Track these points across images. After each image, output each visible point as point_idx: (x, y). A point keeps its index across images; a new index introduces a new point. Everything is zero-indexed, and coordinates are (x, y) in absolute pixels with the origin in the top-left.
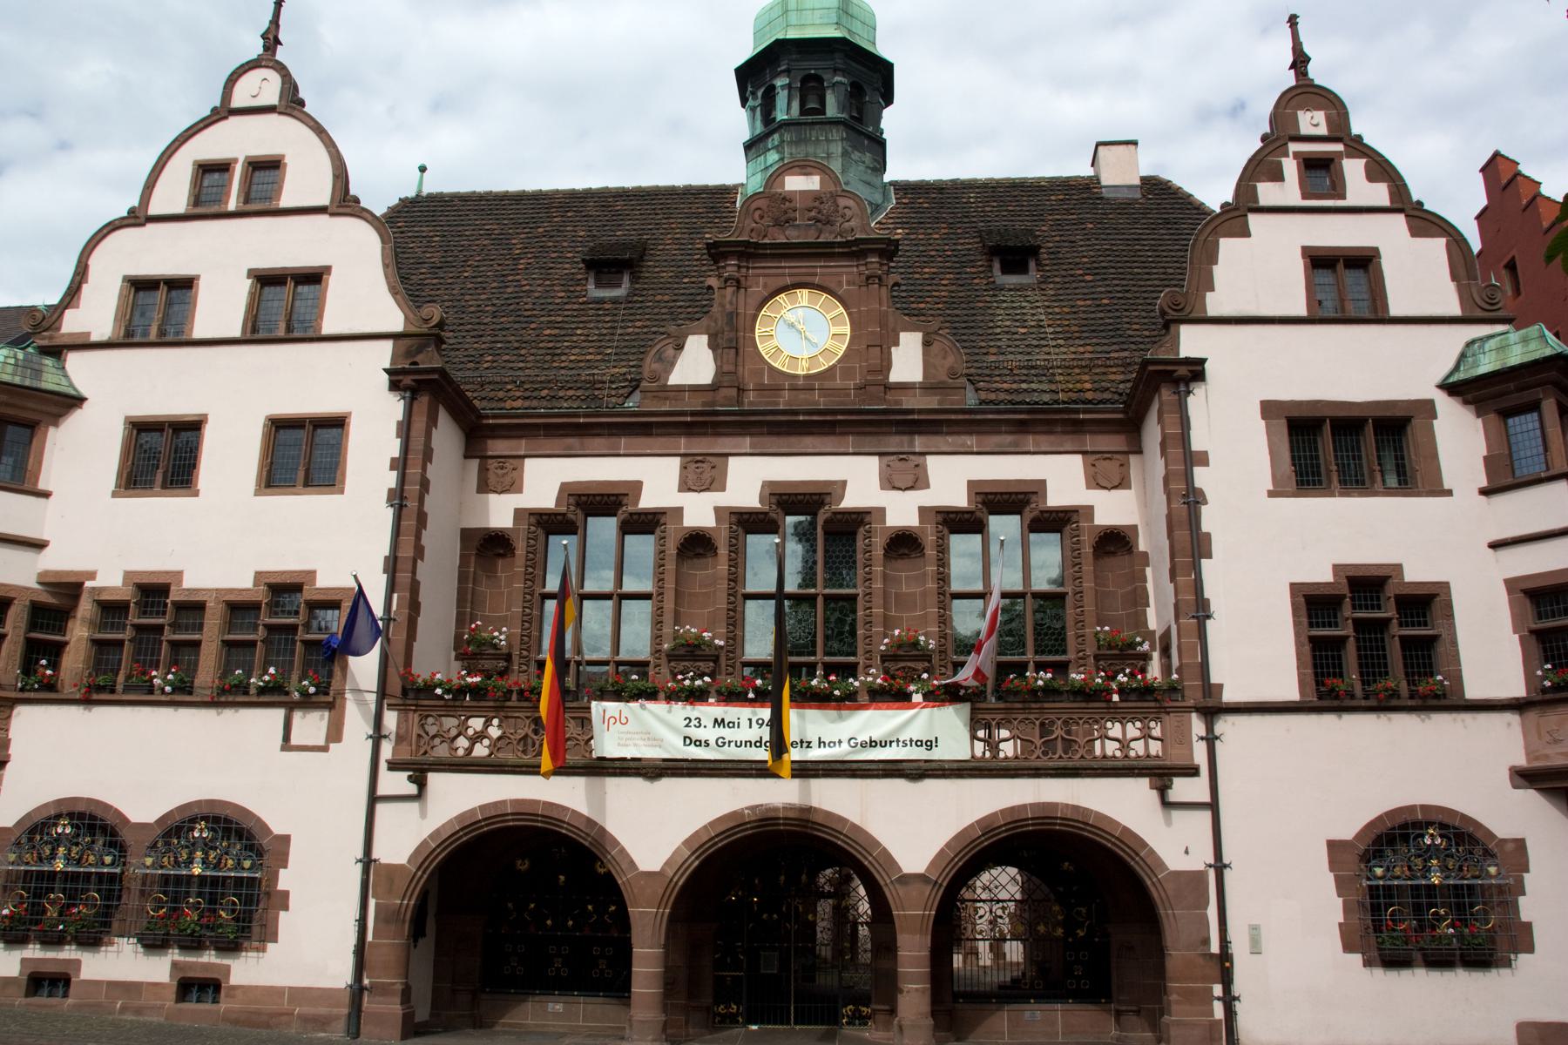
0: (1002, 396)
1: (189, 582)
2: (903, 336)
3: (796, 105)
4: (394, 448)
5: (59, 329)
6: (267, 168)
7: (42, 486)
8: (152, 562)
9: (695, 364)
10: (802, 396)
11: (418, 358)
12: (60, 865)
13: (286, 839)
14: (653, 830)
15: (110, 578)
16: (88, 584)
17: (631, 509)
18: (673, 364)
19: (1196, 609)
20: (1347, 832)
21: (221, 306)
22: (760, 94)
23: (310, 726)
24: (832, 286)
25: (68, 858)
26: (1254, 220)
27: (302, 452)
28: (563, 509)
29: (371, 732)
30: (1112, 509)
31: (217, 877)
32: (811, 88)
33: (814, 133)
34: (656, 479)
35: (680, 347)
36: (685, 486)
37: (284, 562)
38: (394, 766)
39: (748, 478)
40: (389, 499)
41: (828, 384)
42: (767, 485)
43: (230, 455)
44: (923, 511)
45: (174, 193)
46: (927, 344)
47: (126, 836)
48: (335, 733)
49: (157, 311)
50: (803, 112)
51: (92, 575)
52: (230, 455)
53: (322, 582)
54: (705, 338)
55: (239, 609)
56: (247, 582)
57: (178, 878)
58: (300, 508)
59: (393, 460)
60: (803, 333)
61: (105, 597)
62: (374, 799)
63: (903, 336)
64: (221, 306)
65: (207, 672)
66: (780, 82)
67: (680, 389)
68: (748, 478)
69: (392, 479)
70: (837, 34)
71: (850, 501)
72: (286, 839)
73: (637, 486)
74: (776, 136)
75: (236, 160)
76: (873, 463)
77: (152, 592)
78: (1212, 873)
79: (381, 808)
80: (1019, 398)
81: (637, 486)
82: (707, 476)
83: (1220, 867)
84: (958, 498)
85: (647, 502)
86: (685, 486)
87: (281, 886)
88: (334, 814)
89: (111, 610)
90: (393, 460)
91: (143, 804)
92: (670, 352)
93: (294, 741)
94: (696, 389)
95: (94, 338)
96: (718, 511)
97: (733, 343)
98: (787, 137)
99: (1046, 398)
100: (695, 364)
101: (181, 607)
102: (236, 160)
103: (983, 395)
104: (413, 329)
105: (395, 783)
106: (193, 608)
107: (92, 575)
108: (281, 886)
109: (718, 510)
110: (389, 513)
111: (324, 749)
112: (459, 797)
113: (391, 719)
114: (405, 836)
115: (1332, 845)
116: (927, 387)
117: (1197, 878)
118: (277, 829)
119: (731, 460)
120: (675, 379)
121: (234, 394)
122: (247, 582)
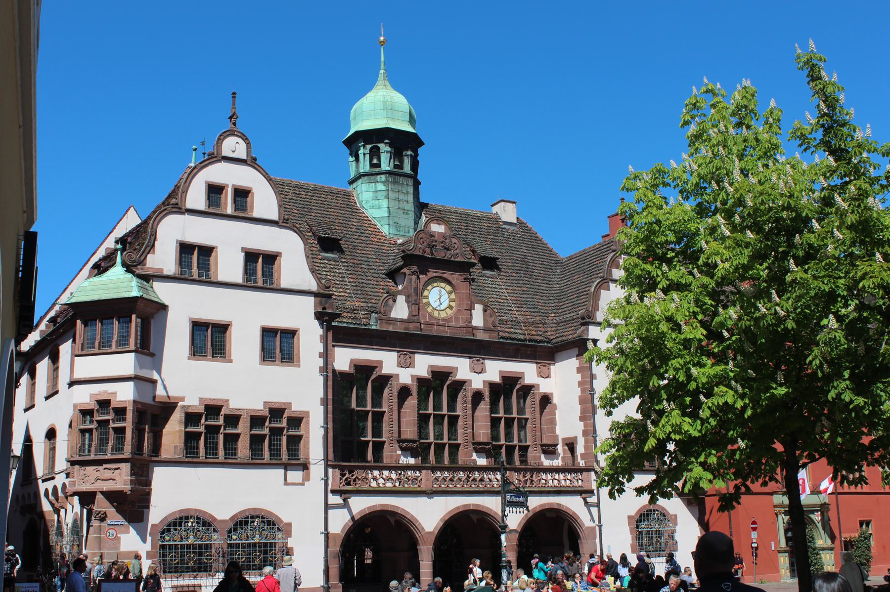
0: (507, 335)
1: (232, 405)
2: (477, 306)
3: (392, 161)
4: (320, 348)
5: (145, 265)
6: (242, 194)
7: (152, 350)
8: (214, 394)
9: (400, 310)
10: (441, 328)
11: (327, 306)
12: (191, 540)
13: (290, 525)
14: (429, 514)
15: (193, 401)
16: (180, 403)
17: (379, 373)
18: (392, 308)
19: (590, 432)
20: (633, 513)
21: (229, 266)
22: (369, 147)
23: (295, 476)
24: (451, 280)
25: (195, 536)
26: (612, 285)
27: (278, 344)
28: (352, 371)
29: (323, 477)
30: (545, 386)
31: (255, 543)
32: (397, 154)
33: (401, 179)
34: (388, 361)
35: (395, 301)
36: (400, 365)
37: (278, 398)
38: (334, 492)
39: (424, 364)
40: (320, 371)
41: (450, 324)
42: (430, 366)
43: (244, 342)
44: (484, 382)
45: (196, 197)
46: (485, 311)
47: (215, 525)
48: (307, 478)
49: (196, 260)
50: (395, 166)
51: (183, 399)
52: (244, 342)
53: (294, 409)
54: (404, 297)
55: (256, 421)
56: (262, 408)
57: (249, 545)
58: (278, 371)
59: (320, 353)
60: (439, 298)
61: (190, 410)
62: (327, 507)
63: (477, 306)
64: (229, 266)
65: (243, 448)
66: (384, 148)
67: (396, 320)
68: (424, 364)
69: (320, 362)
70: (410, 129)
71: (460, 376)
72: (290, 525)
73: (381, 363)
74: (383, 177)
75: (228, 186)
76: (467, 361)
77: (213, 410)
78: (597, 528)
79: (330, 511)
80: (513, 336)
81: (381, 363)
82: (409, 361)
83: (600, 527)
84: (496, 379)
85: (385, 371)
86: (400, 365)
87: (289, 546)
88: (307, 511)
89: (191, 418)
90: (320, 353)
91: (223, 511)
92: (391, 301)
93: (289, 481)
94: (403, 321)
95: (166, 272)
96: (412, 376)
97: (415, 300)
98: (390, 179)
99: (522, 337)
100: (400, 310)
101: (227, 417)
102: (228, 186)
103: (501, 334)
104: (322, 291)
105: (335, 499)
106: (233, 420)
107: (183, 399)
108: (289, 546)
109: (412, 376)
110: (322, 379)
111: (303, 484)
112: (360, 505)
113: (330, 470)
114: (340, 522)
115: (629, 517)
116: (486, 330)
117: (594, 528)
118: (285, 520)
119: (417, 356)
120: (393, 315)
121: (247, 315)
122: (262, 408)
